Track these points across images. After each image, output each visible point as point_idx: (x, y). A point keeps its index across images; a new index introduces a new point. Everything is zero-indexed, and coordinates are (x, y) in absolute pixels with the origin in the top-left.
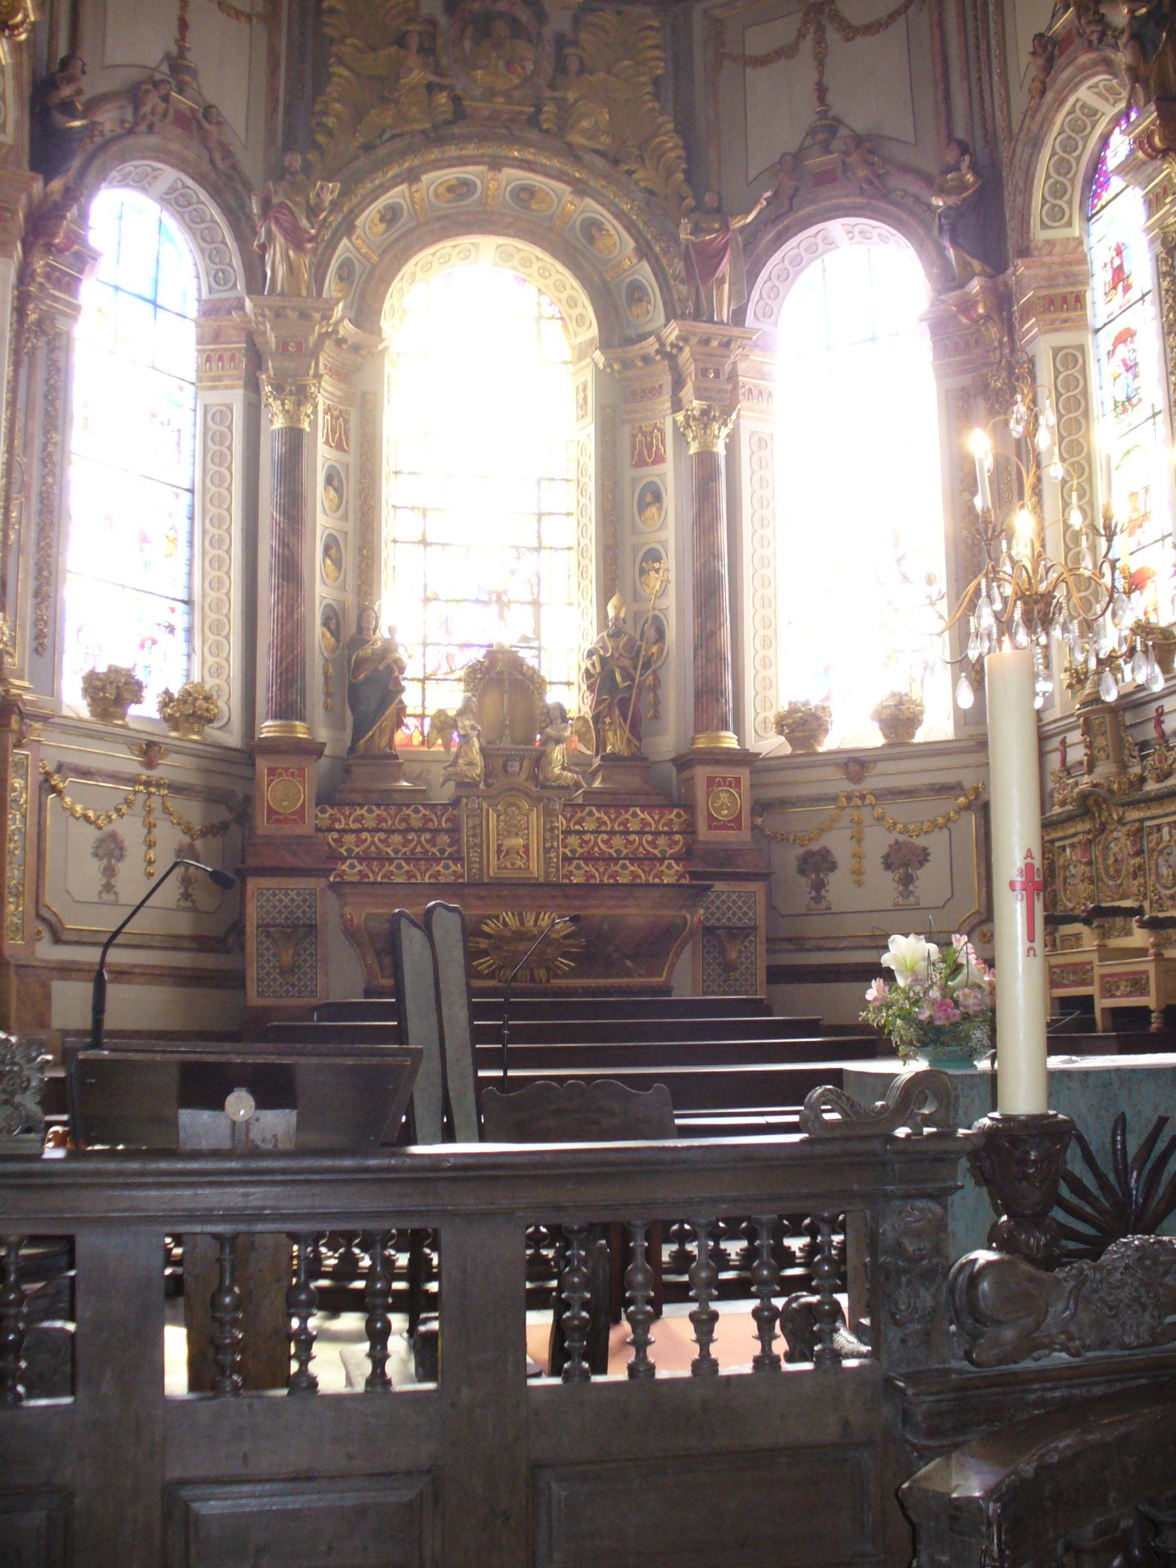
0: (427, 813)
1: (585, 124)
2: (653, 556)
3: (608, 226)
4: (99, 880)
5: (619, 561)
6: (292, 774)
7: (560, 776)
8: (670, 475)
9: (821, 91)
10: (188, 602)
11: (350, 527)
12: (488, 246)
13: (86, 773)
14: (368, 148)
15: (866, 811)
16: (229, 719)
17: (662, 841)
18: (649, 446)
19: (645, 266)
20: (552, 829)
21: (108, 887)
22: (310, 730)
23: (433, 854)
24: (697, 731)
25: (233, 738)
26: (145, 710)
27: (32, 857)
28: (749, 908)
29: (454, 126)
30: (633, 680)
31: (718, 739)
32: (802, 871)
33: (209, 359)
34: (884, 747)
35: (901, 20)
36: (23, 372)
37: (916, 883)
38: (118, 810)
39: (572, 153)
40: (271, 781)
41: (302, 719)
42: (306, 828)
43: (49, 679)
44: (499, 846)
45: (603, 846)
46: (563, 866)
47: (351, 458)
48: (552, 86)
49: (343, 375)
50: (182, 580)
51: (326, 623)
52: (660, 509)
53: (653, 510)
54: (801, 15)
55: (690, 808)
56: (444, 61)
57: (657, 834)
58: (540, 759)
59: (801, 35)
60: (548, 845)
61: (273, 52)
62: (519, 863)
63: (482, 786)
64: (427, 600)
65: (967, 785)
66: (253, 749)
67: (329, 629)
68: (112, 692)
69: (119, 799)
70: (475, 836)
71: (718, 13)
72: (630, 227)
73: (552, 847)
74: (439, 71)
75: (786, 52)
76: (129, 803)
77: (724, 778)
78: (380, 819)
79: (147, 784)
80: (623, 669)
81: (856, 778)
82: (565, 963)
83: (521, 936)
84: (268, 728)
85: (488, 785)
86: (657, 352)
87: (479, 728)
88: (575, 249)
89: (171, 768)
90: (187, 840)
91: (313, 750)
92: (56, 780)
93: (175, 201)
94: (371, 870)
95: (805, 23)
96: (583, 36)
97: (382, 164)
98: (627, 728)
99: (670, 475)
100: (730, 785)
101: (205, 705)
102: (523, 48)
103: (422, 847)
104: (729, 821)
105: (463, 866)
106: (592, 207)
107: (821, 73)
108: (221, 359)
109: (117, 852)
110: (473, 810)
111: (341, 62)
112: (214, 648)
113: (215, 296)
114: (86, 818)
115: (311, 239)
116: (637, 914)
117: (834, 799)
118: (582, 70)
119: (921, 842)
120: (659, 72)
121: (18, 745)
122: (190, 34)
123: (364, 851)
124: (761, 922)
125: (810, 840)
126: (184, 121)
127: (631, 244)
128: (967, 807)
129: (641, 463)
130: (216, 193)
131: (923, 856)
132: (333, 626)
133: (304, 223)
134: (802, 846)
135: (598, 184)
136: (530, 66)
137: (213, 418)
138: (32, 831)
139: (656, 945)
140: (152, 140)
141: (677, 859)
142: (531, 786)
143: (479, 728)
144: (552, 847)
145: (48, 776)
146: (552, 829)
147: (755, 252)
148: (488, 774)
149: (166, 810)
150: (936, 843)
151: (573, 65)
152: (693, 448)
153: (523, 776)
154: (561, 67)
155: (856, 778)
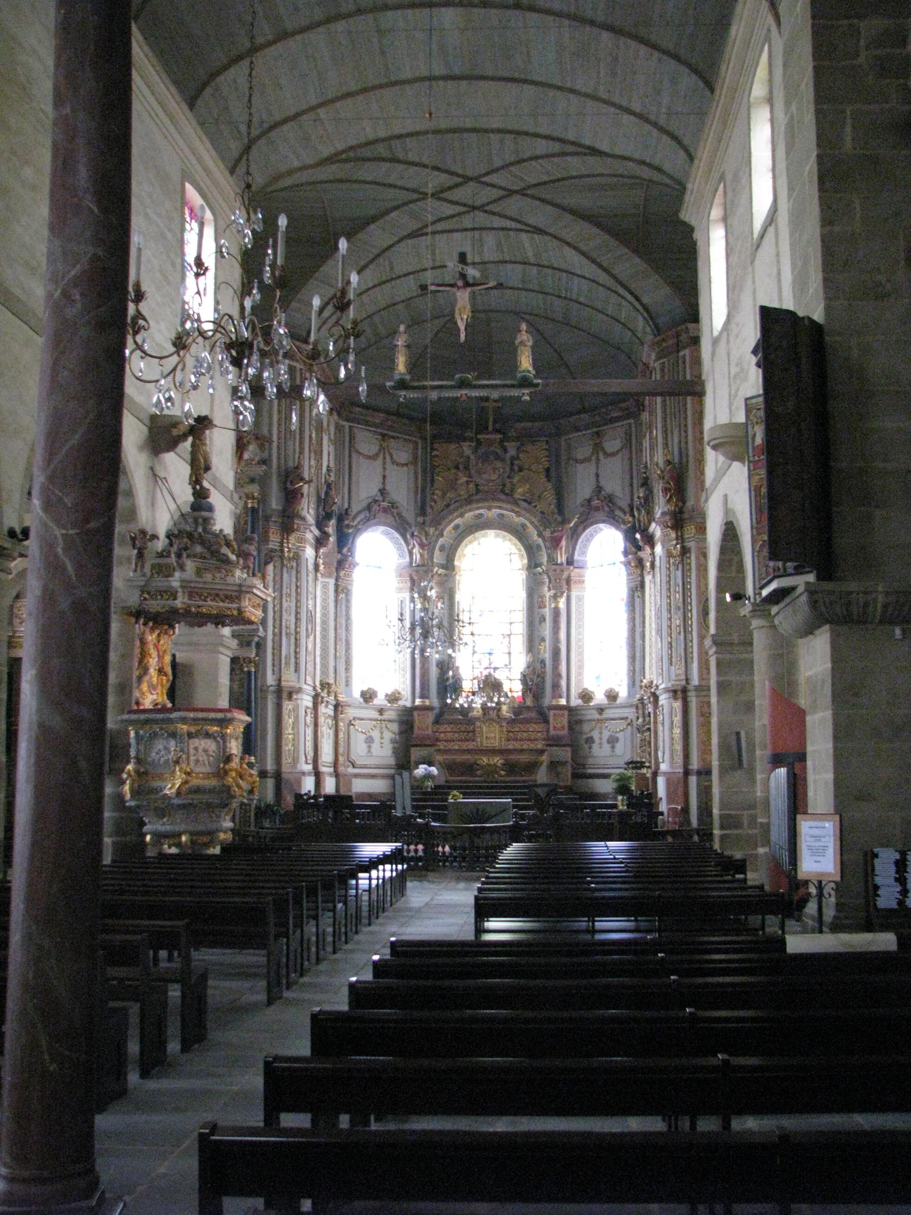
1: (520, 490)
5: (532, 642)
8: (547, 612)
9: (597, 475)
12: (491, 533)
13: (362, 719)
14: (448, 506)
17: (539, 734)
21: (369, 751)
25: (408, 704)
26: (380, 700)
29: (478, 495)
39: (516, 503)
42: (429, 732)
43: (350, 694)
48: (509, 477)
49: (441, 584)
51: (437, 666)
53: (543, 624)
56: (472, 472)
61: (416, 473)
66: (415, 708)
68: (368, 696)
69: (372, 726)
71: (569, 441)
72: (536, 527)
74: (470, 476)
81: (601, 714)
82: (503, 773)
83: (489, 765)
84: (418, 702)
88: (519, 533)
89: (386, 716)
91: (429, 708)
92: (353, 722)
93: (387, 534)
96: (521, 455)
97: (451, 513)
102: (499, 464)
106: (522, 520)
111: (438, 475)
116: (524, 758)
118: (521, 470)
119: (617, 735)
120: (546, 466)
122: (386, 481)
124: (570, 760)
126: (385, 510)
127: (536, 533)
128: (629, 724)
129: (540, 607)
131: (617, 740)
135: (524, 512)
136: (501, 470)
139: (532, 767)
140: (375, 521)
147: (575, 535)
148: (484, 714)
150: (620, 735)
151: (516, 468)
152: (553, 606)
154: (512, 469)
155: (601, 714)
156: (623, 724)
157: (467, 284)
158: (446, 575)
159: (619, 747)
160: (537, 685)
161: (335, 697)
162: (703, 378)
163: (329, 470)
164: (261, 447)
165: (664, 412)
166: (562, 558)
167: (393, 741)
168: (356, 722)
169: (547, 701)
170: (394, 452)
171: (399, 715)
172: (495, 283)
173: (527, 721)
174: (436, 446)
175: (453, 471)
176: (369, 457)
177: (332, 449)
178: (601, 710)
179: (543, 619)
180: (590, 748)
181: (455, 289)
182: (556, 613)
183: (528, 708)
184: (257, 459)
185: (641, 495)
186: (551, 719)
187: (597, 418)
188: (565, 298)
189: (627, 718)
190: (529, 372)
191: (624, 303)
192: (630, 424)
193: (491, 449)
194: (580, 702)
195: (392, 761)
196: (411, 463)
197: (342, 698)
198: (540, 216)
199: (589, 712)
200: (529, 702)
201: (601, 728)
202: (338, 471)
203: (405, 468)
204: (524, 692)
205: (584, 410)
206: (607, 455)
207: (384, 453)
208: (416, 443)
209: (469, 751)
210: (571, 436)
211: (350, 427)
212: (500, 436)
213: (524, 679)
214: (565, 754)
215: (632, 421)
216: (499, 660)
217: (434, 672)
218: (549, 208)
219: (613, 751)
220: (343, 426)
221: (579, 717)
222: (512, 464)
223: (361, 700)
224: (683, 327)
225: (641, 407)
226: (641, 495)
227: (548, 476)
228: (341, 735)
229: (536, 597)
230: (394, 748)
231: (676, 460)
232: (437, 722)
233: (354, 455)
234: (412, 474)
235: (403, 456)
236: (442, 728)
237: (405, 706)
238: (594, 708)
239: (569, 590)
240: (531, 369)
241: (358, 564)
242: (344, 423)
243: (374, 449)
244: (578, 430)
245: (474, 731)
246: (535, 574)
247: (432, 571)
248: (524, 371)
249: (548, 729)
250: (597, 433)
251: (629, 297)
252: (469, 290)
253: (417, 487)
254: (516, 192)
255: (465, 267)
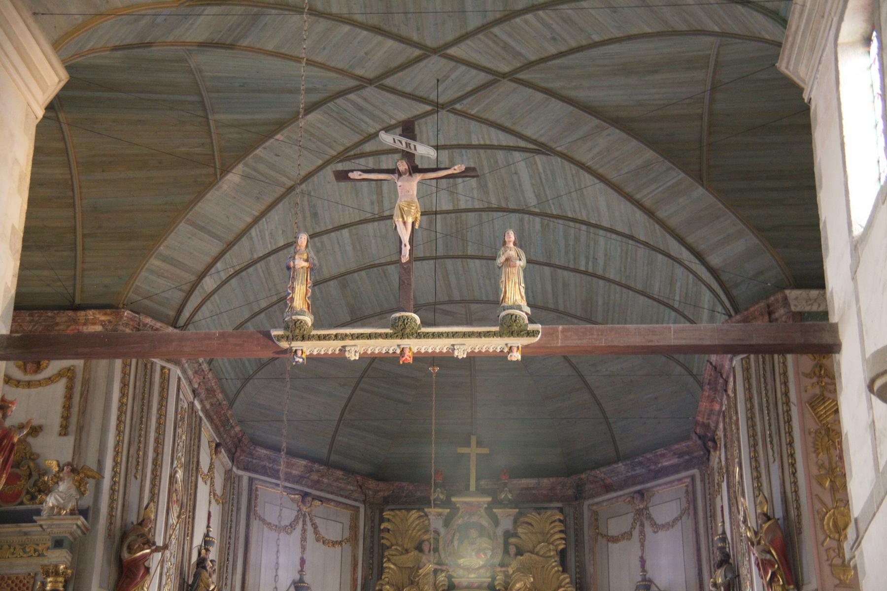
9: (643, 561)
35: (679, 524)
54: (632, 514)
59: (633, 528)
71: (595, 508)
75: (627, 536)
95: (635, 520)
96: (520, 530)
107: (643, 551)
111: (389, 560)
120: (562, 547)
157: (414, 169)
162: (834, 318)
163: (207, 542)
164: (80, 487)
165: (753, 436)
170: (318, 521)
172: (463, 168)
174: (387, 514)
175: (414, 553)
176: (278, 528)
177: (216, 510)
181: (394, 177)
184: (70, 506)
185: (720, 581)
187: (639, 470)
188: (586, 273)
190: (519, 308)
191: (679, 271)
192: (693, 478)
193: (474, 519)
196: (348, 540)
198: (543, 120)
202: (226, 550)
203: (338, 549)
205: (618, 459)
206: (657, 528)
207: (304, 523)
208: (358, 508)
210: (596, 500)
211: (251, 480)
212: (489, 499)
215: (695, 471)
218: (557, 105)
220: (240, 477)
222: (506, 544)
224: (779, 296)
225: (710, 444)
226: (720, 581)
227: (563, 562)
231: (779, 513)
233: (255, 524)
234: (348, 559)
235: (334, 530)
240: (523, 303)
242: (240, 473)
243: (289, 515)
244: (608, 488)
248: (511, 307)
250: (641, 493)
251: (685, 255)
252: (418, 177)
253: (354, 580)
254: (504, 75)
255: (412, 143)
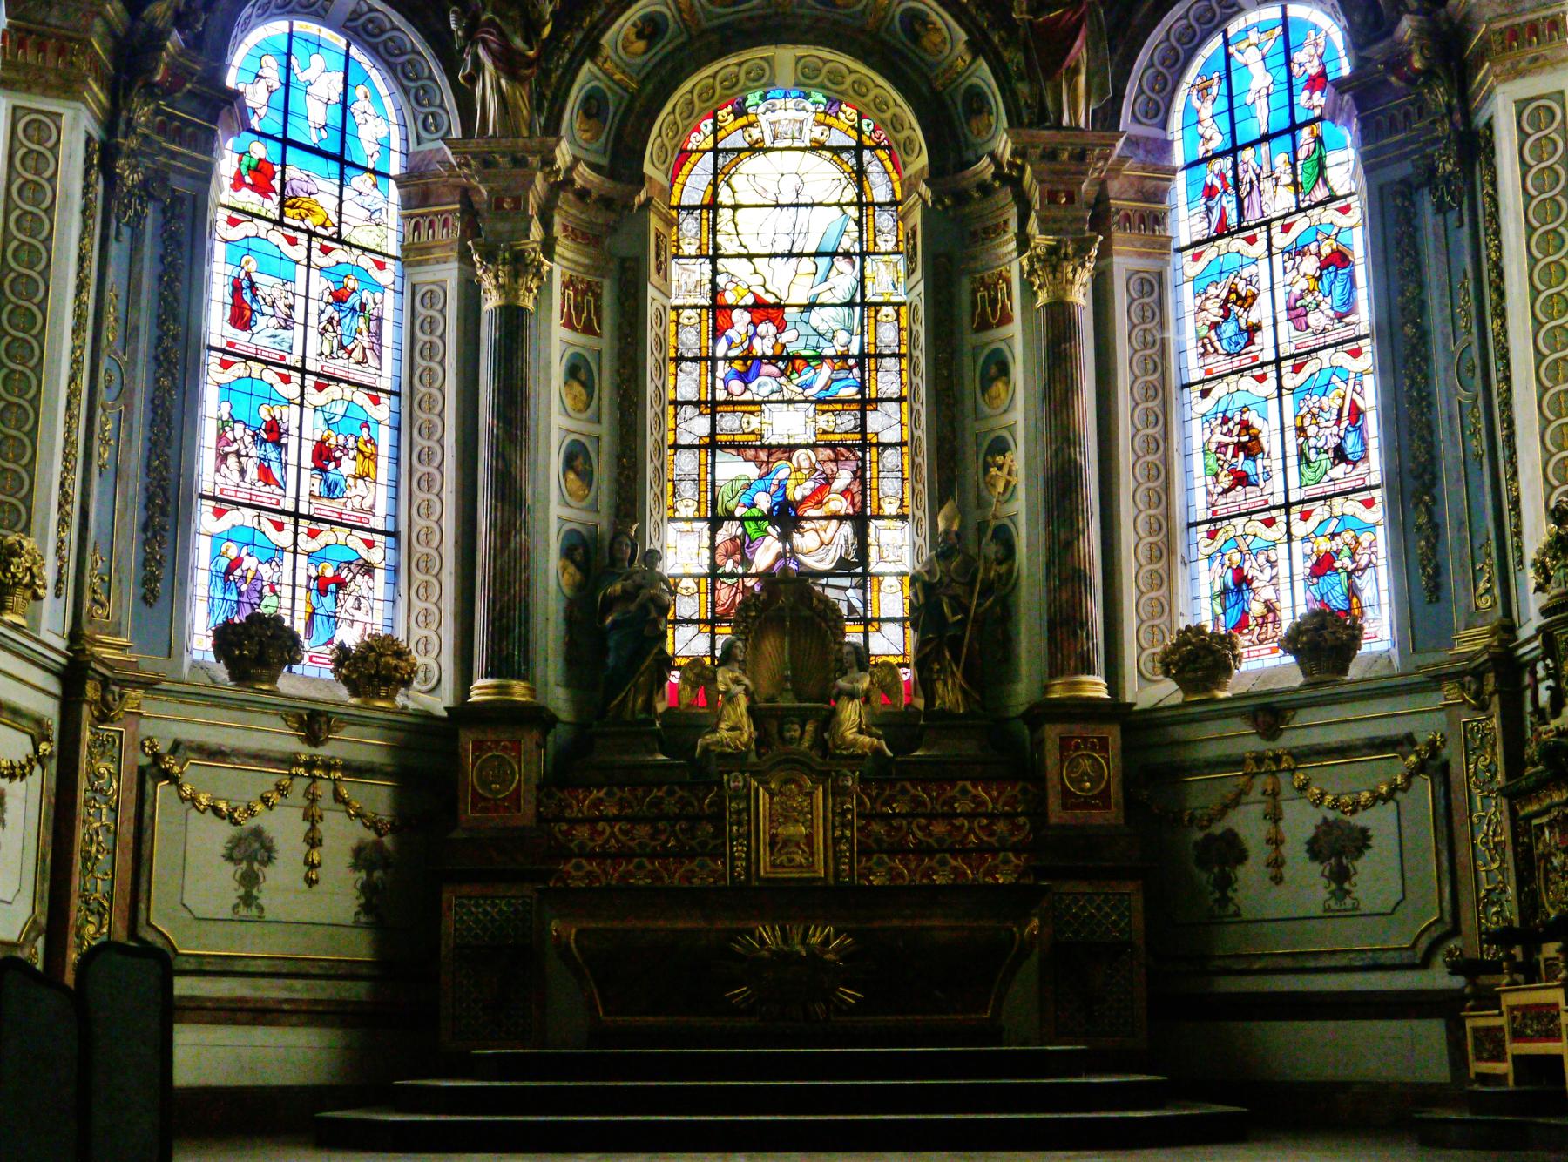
0: (686, 794)
2: (1000, 447)
3: (934, 17)
4: (233, 892)
6: (505, 748)
7: (853, 744)
8: (1017, 338)
10: (394, 534)
11: (604, 430)
15: (1284, 778)
16: (439, 680)
18: (993, 302)
19: (983, 67)
20: (844, 812)
21: (248, 900)
22: (532, 691)
23: (691, 848)
24: (1052, 676)
25: (440, 703)
26: (311, 675)
27: (125, 862)
28: (1121, 916)
30: (966, 611)
31: (1076, 685)
32: (1203, 863)
33: (417, 227)
34: (1303, 686)
36: (117, 250)
37: (1354, 879)
38: (264, 800)
40: (477, 758)
41: (523, 678)
43: (170, 638)
44: (773, 837)
45: (919, 834)
46: (859, 862)
47: (605, 343)
50: (382, 508)
51: (568, 552)
52: (1007, 383)
53: (999, 387)
55: (1040, 780)
57: (993, 817)
58: (829, 720)
60: (838, 833)
62: (799, 858)
63: (753, 758)
64: (715, 523)
65: (1422, 738)
66: (464, 713)
67: (573, 561)
68: (255, 646)
70: (739, 824)
73: (843, 836)
76: (281, 790)
77: (1085, 739)
78: (622, 804)
79: (310, 765)
80: (954, 598)
82: (849, 995)
83: (784, 958)
84: (481, 689)
85: (759, 755)
86: (995, 176)
87: (747, 681)
89: (344, 745)
90: (371, 836)
91: (536, 717)
92: (169, 762)
94: (604, 871)
98: (959, 675)
99: (1017, 338)
100: (1093, 747)
101: (393, 662)
103: (678, 840)
104: (1094, 797)
105: (724, 864)
108: (431, 225)
109: (262, 854)
110: (736, 789)
112: (422, 591)
113: (426, 146)
114: (216, 811)
115: (530, 63)
117: (1238, 763)
119: (1360, 819)
121: (104, 718)
123: (601, 846)
125: (1211, 821)
127: (962, 36)
128: (1421, 768)
129: (984, 326)
130: (411, 16)
131: (1362, 840)
132: (578, 558)
133: (518, 42)
134: (1202, 828)
137: (417, 299)
138: (127, 830)
141: (1017, 851)
142: (816, 755)
143: (747, 681)
144: (843, 836)
145: (157, 757)
146: (844, 812)
148: (762, 741)
149: (337, 797)
152: (1042, 298)
153: (806, 743)
156: (1395, 768)
158: (606, 202)
159: (1375, 877)
160: (980, 622)
161: (75, 636)
166: (1079, 111)
167: (363, 857)
168: (193, 774)
169: (1023, 692)
171: (395, 749)
173: (942, 774)
178: (1268, 712)
179: (999, 367)
180: (1225, 882)
182: (1059, 319)
183: (939, 720)
186: (1052, 761)
189: (1409, 739)
194: (1166, 691)
195: (359, 947)
197: (108, 650)
199: (1212, 729)
200: (949, 696)
201: (1275, 794)
204: (924, 660)
209: (696, 899)
213: (927, 611)
214: (1120, 909)
216: (820, 546)
217: (551, 577)
219: (1341, 893)
221: (1161, 757)
223: (222, 672)
228: (96, 822)
229: (966, 283)
230: (367, 889)
232: (565, 773)
236: (584, 802)
237: (428, 716)
238: (1230, 710)
239: (1105, 252)
241: (234, 97)
245: (718, 818)
246: (961, 198)
247: (548, 161)
249: (1042, 801)
